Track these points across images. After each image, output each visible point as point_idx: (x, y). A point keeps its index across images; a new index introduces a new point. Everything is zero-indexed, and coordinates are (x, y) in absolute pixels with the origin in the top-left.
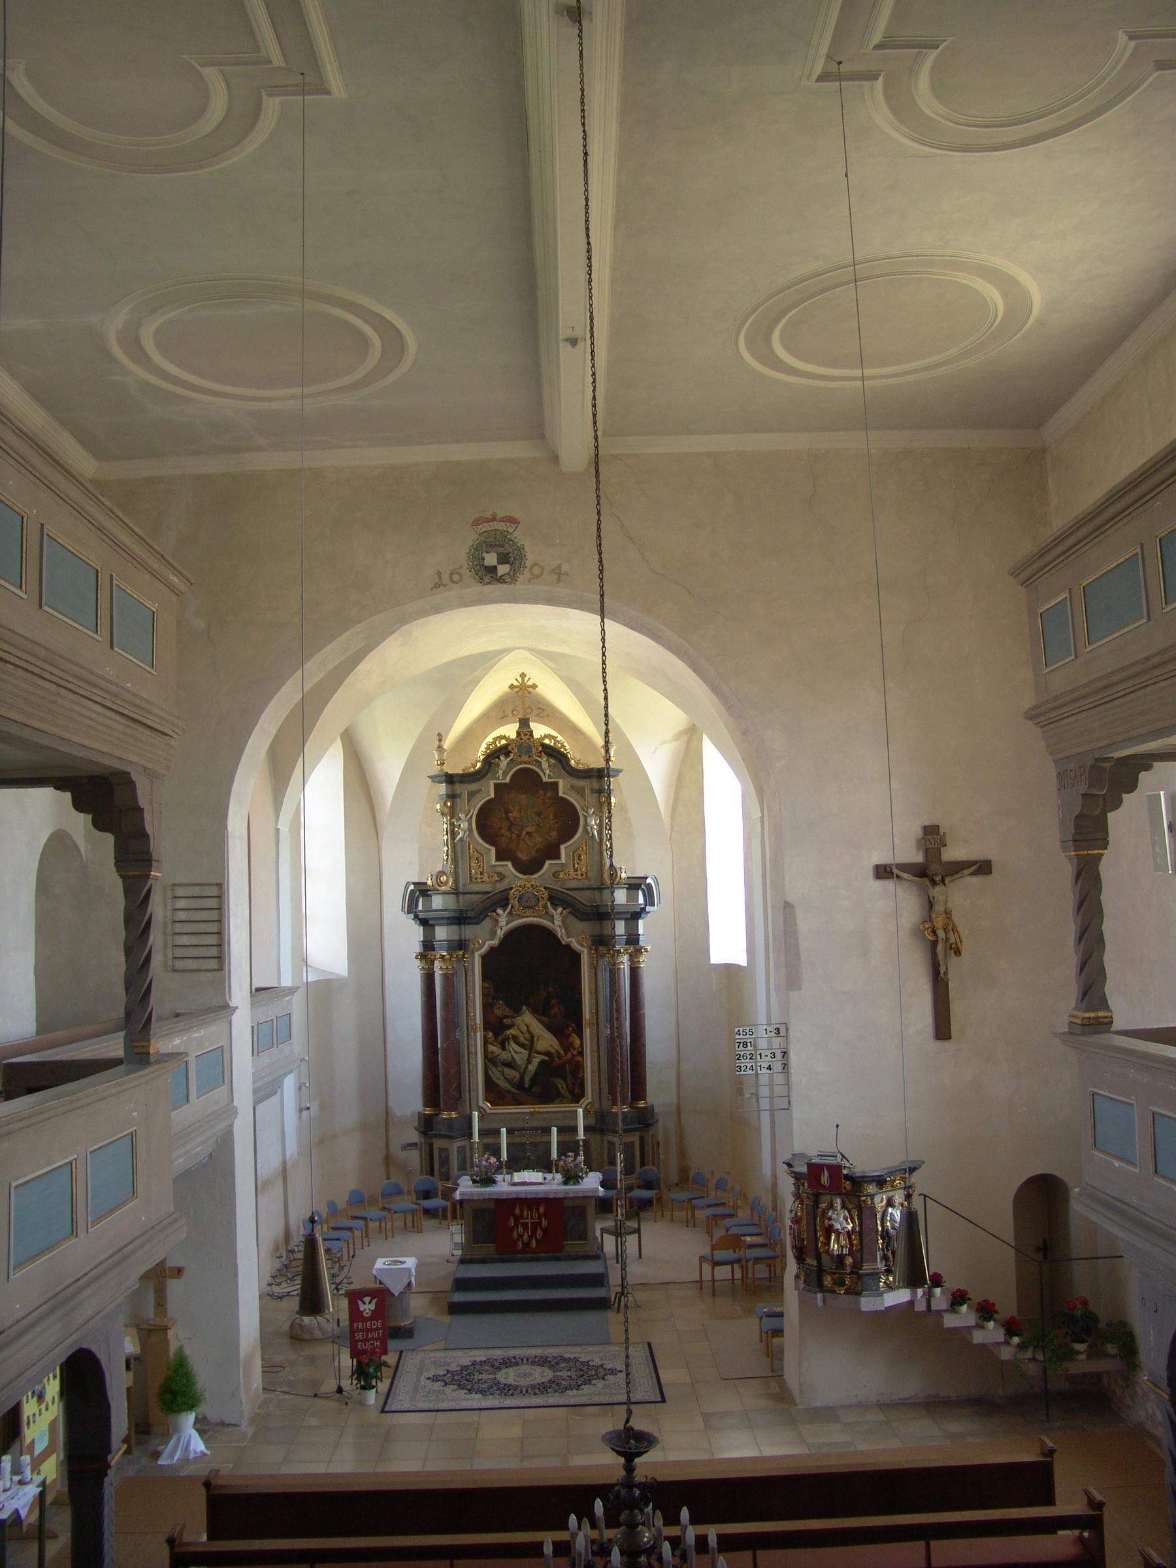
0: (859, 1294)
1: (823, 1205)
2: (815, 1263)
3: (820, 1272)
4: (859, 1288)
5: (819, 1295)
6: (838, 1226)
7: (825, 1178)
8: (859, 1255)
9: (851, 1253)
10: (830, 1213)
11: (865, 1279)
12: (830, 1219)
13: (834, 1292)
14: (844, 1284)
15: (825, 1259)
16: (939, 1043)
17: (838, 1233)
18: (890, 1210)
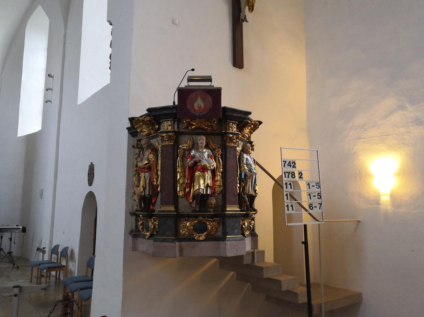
0: (223, 239)
1: (184, 146)
2: (172, 208)
3: (179, 217)
4: (220, 234)
5: (177, 244)
6: (204, 163)
7: (199, 104)
8: (220, 197)
9: (213, 194)
10: (193, 153)
11: (230, 222)
12: (193, 157)
13: (193, 240)
14: (206, 229)
15: (183, 203)
16: (236, 70)
17: (204, 169)
18: (245, 156)
